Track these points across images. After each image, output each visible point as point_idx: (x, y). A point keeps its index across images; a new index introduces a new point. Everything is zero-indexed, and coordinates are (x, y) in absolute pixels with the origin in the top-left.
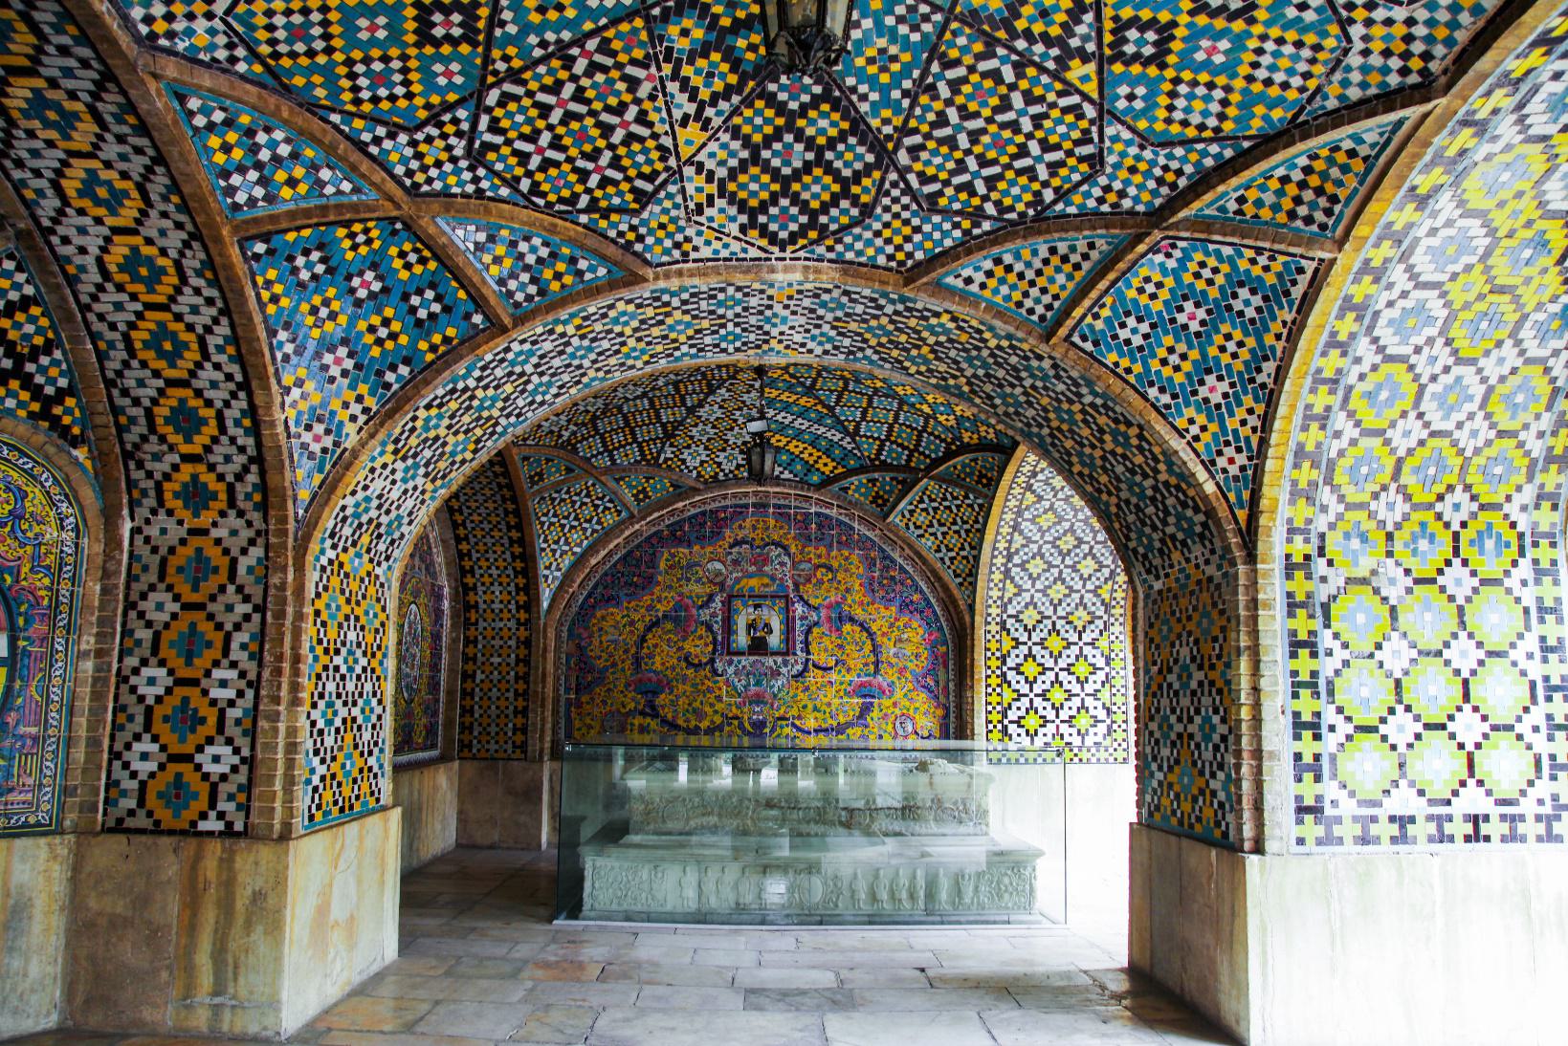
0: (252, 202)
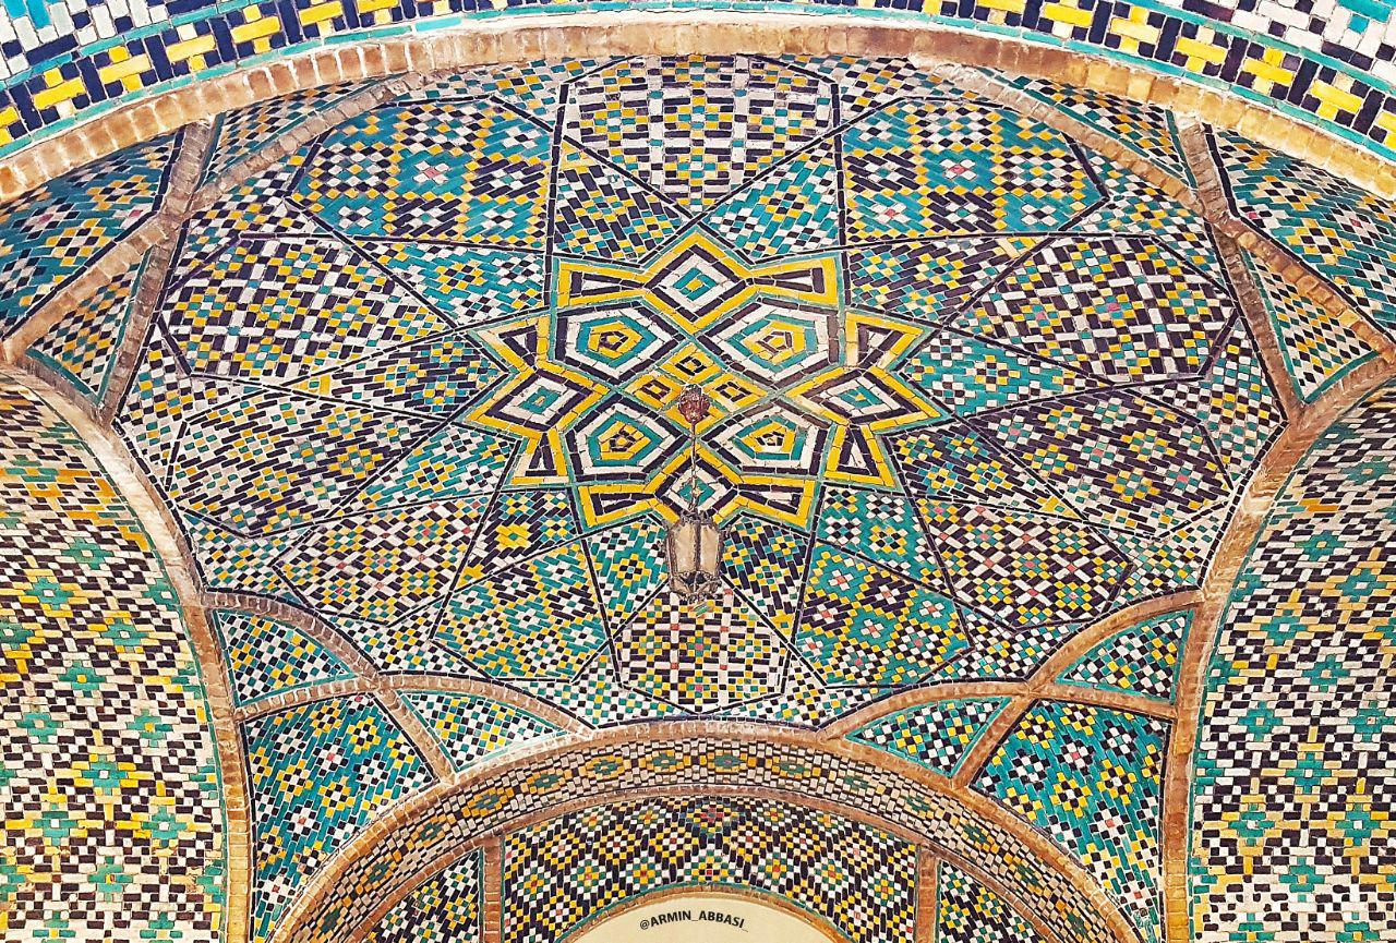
0: (952, 759)
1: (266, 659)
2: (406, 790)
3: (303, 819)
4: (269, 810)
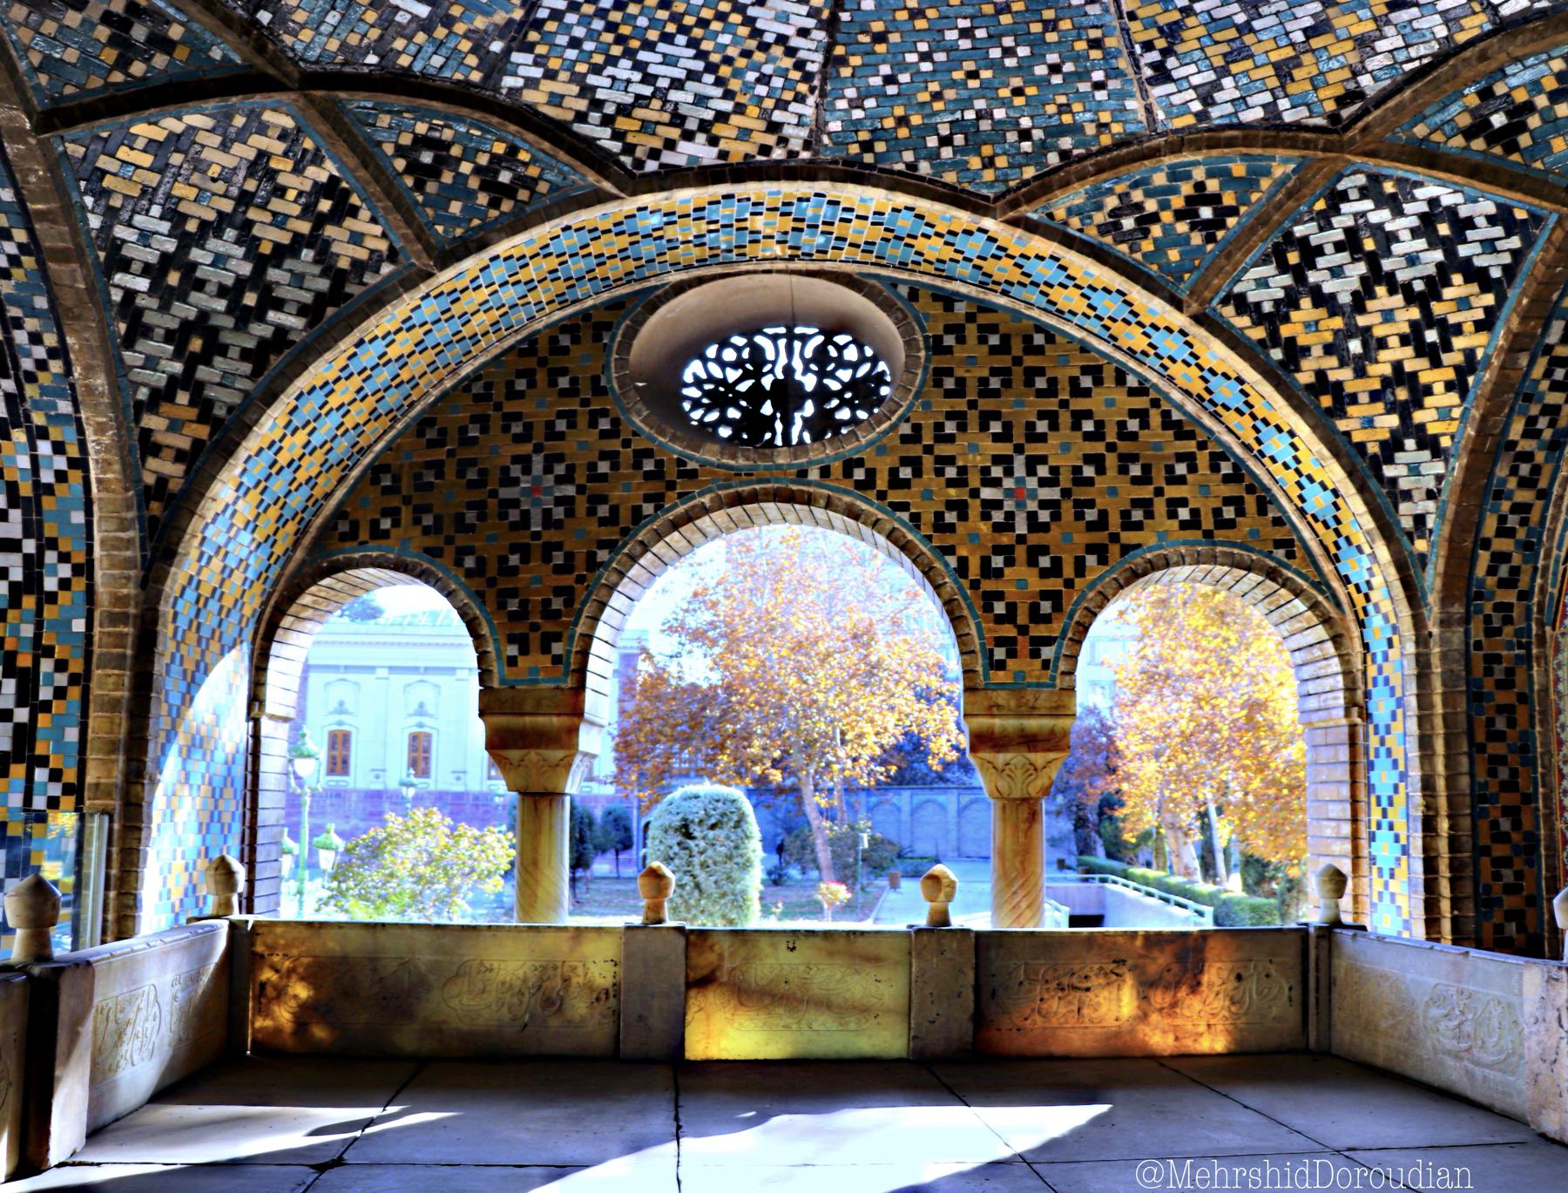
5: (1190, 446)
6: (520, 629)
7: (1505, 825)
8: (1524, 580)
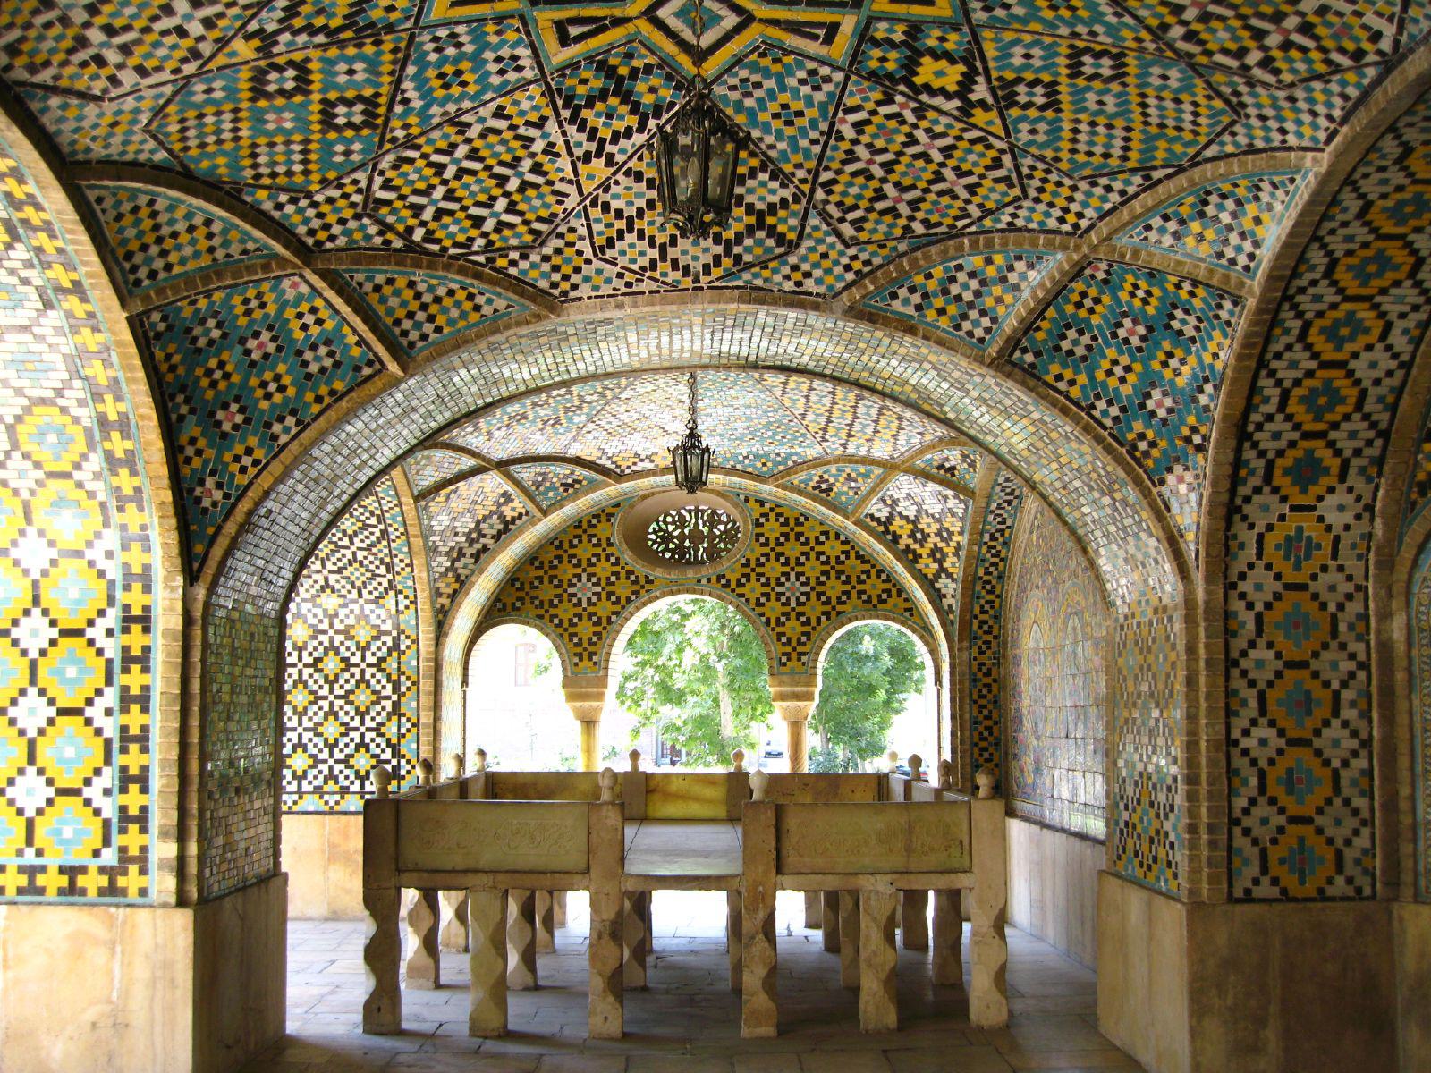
1: (968, 297)
2: (1228, 323)
3: (1159, 402)
4: (1114, 411)
5: (867, 567)
6: (579, 650)
7: (986, 734)
8: (995, 632)
